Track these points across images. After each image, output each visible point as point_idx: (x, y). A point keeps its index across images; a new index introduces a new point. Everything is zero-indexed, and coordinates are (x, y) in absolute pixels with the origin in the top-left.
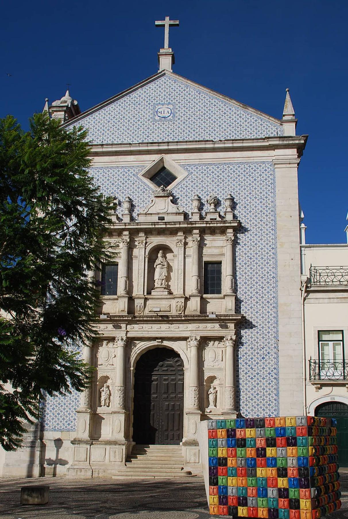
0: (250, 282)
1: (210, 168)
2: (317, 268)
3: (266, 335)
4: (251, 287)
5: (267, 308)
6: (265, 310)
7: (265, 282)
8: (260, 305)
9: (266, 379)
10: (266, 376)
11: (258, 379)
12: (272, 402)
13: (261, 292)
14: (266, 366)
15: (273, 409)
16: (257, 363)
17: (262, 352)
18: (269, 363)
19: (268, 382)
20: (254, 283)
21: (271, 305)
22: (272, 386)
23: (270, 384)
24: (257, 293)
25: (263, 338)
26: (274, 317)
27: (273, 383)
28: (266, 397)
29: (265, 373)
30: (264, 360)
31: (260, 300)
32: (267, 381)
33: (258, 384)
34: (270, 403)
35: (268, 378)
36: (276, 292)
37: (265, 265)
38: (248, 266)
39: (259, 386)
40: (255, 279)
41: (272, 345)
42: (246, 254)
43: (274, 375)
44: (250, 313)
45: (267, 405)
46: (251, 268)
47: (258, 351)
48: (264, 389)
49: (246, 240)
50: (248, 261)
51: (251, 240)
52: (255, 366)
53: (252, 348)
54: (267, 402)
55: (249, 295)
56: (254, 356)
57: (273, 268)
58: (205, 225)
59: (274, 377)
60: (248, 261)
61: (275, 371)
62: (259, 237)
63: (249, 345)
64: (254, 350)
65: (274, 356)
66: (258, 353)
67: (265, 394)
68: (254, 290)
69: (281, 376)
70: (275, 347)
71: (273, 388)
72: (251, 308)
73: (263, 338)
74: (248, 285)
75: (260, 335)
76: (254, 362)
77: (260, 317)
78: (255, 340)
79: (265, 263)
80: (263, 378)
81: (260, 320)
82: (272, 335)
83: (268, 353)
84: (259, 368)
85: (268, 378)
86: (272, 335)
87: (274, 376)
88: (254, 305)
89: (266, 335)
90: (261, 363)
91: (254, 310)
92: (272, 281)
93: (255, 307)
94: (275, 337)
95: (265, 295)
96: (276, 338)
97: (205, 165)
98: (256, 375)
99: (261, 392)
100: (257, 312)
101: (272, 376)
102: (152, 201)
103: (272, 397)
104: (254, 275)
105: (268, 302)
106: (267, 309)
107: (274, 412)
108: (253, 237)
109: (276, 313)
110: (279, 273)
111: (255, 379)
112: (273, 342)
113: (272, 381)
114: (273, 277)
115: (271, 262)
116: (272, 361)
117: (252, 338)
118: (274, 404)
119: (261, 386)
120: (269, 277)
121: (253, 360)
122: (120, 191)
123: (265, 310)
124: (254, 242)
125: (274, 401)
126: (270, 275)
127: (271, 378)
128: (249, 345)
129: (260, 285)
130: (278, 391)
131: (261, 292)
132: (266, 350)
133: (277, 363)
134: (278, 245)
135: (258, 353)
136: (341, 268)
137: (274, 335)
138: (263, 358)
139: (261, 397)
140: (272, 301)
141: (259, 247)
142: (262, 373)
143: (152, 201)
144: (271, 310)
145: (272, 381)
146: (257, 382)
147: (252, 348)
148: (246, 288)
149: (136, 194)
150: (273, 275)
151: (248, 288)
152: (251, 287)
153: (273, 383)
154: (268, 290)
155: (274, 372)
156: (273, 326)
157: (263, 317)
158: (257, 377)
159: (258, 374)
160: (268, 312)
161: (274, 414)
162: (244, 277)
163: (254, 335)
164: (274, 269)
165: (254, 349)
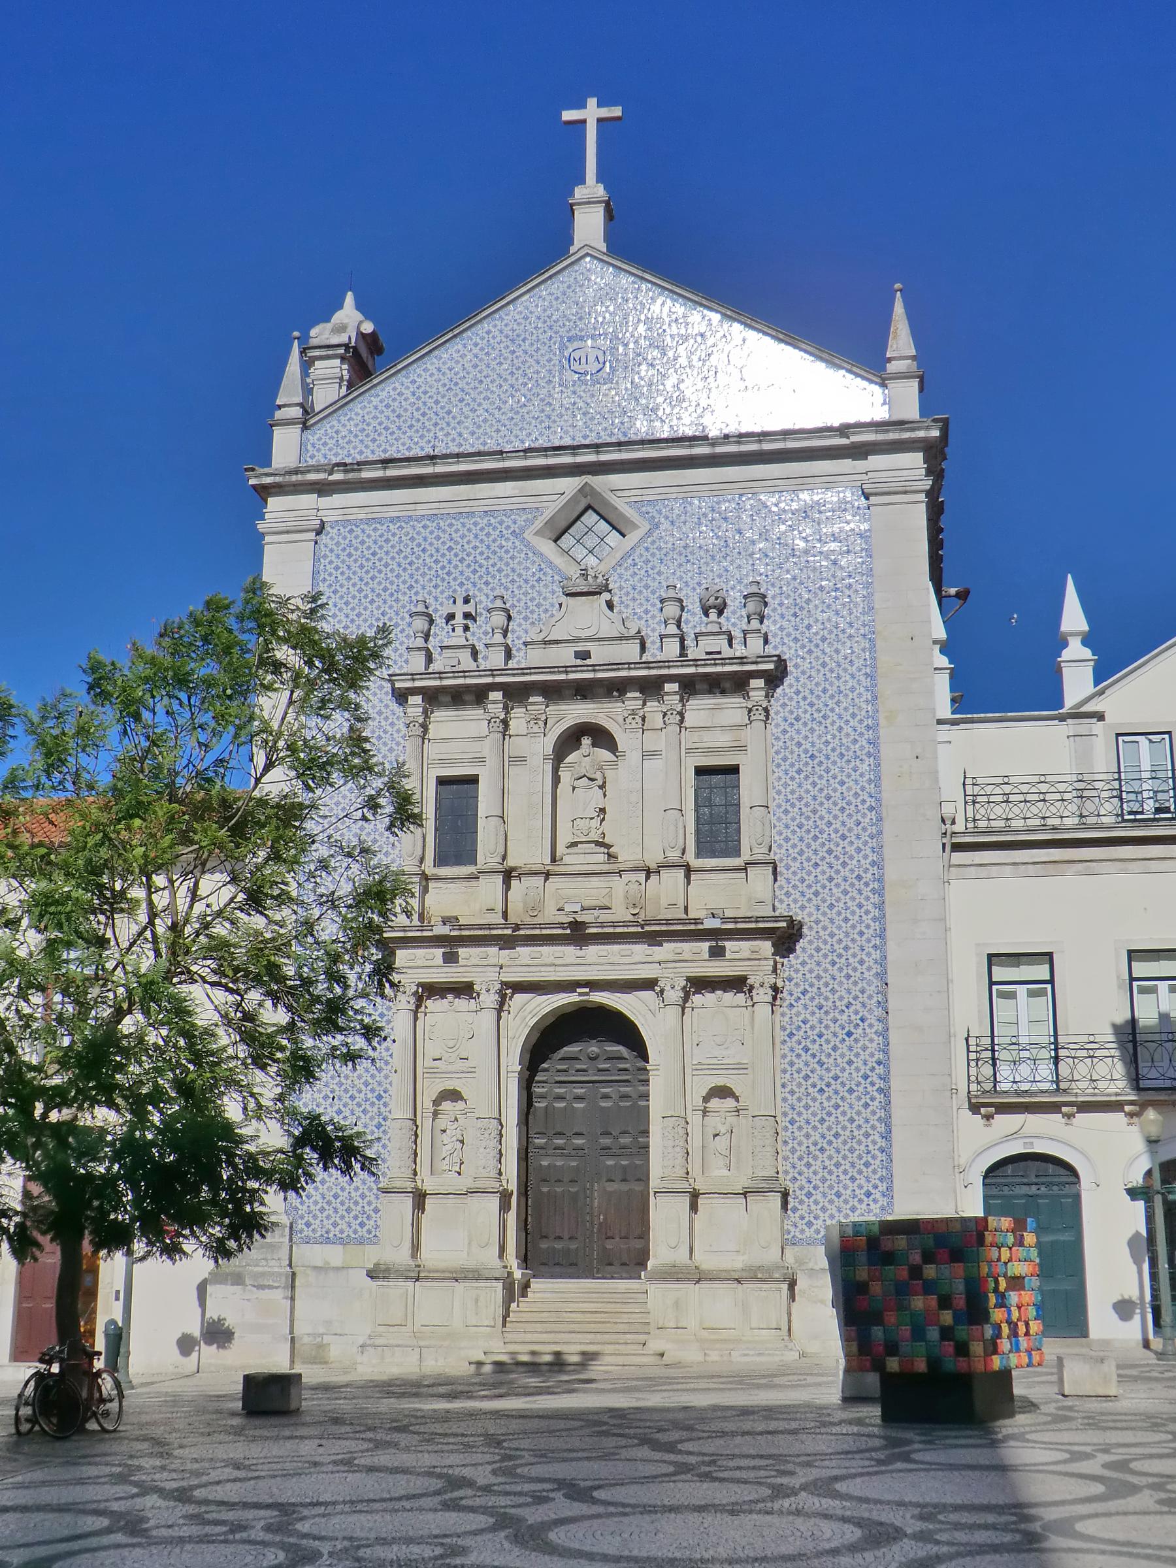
0: (811, 823)
2: (979, 781)
3: (855, 969)
4: (815, 838)
5: (855, 893)
6: (853, 899)
7: (850, 823)
8: (838, 885)
9: (856, 1094)
10: (859, 1084)
11: (836, 1092)
12: (874, 1157)
13: (840, 849)
14: (857, 1055)
15: (877, 1176)
16: (835, 1049)
17: (845, 1017)
18: (864, 1048)
19: (863, 1101)
20: (822, 824)
21: (867, 884)
22: (874, 1113)
23: (866, 1105)
24: (830, 852)
25: (848, 977)
26: (874, 919)
27: (876, 1103)
28: (859, 1142)
29: (855, 1075)
30: (852, 1038)
31: (837, 872)
32: (859, 1099)
33: (837, 1107)
34: (870, 1159)
35: (861, 1089)
36: (878, 850)
37: (849, 776)
38: (807, 777)
39: (839, 1111)
40: (824, 813)
41: (870, 997)
42: (799, 745)
43: (878, 1081)
44: (813, 910)
45: (860, 1165)
46: (814, 784)
47: (837, 1015)
48: (852, 1121)
49: (799, 707)
50: (807, 764)
51: (811, 704)
52: (829, 1055)
53: (820, 1007)
54: (860, 1157)
55: (809, 860)
56: (827, 1027)
57: (870, 781)
58: (692, 670)
59: (877, 1086)
61: (880, 1070)
62: (832, 697)
63: (812, 999)
64: (826, 1013)
65: (876, 1028)
66: (835, 1021)
67: (856, 1133)
68: (823, 845)
69: (895, 1084)
70: (879, 1002)
71: (876, 1117)
72: (816, 894)
73: (848, 977)
74: (808, 831)
75: (840, 970)
76: (825, 1047)
77: (838, 921)
78: (826, 984)
79: (848, 769)
80: (851, 1091)
81: (839, 928)
82: (869, 969)
83: (862, 1020)
84: (839, 1060)
85: (861, 1089)
86: (869, 969)
87: (880, 1084)
88: (824, 887)
89: (855, 969)
90: (843, 1048)
91: (824, 901)
92: (867, 820)
93: (827, 891)
94: (877, 974)
95: (851, 858)
96: (882, 976)
98: (833, 1082)
99: (844, 1128)
100: (831, 906)
101: (873, 1084)
102: (560, 605)
103: (874, 1143)
104: (821, 804)
105: (859, 877)
106: (858, 897)
107: (880, 1184)
108: (818, 697)
109: (881, 906)
110: (885, 795)
111: (830, 1092)
112: (873, 988)
113: (873, 1099)
114: (871, 808)
115: (865, 767)
116: (871, 1041)
117: (819, 977)
118: (878, 1162)
119: (844, 1113)
120: (860, 807)
121: (823, 1039)
122: (481, 577)
123: (853, 899)
124: (819, 711)
125: (879, 1154)
126: (864, 802)
127: (870, 1089)
128: (812, 999)
129: (836, 831)
130: (888, 1126)
131: (840, 849)
132: (857, 1013)
133: (885, 1049)
134: (882, 722)
135: (835, 1021)
136: (1043, 779)
137: (876, 968)
138: (849, 1034)
139: (845, 1143)
140: (869, 875)
141: (833, 723)
142: (846, 1074)
143: (560, 605)
144: (868, 898)
145: (873, 1099)
146: (833, 1101)
147: (820, 1007)
148: (801, 839)
149: (520, 587)
150: (871, 802)
151: (808, 838)
152: (815, 838)
153: (876, 1103)
154: (858, 843)
155: (877, 1071)
156: (873, 943)
157: (846, 920)
158: (833, 1087)
159: (836, 1078)
160: (860, 906)
161: (880, 1189)
163: (826, 971)
164: (873, 786)
165: (825, 1009)
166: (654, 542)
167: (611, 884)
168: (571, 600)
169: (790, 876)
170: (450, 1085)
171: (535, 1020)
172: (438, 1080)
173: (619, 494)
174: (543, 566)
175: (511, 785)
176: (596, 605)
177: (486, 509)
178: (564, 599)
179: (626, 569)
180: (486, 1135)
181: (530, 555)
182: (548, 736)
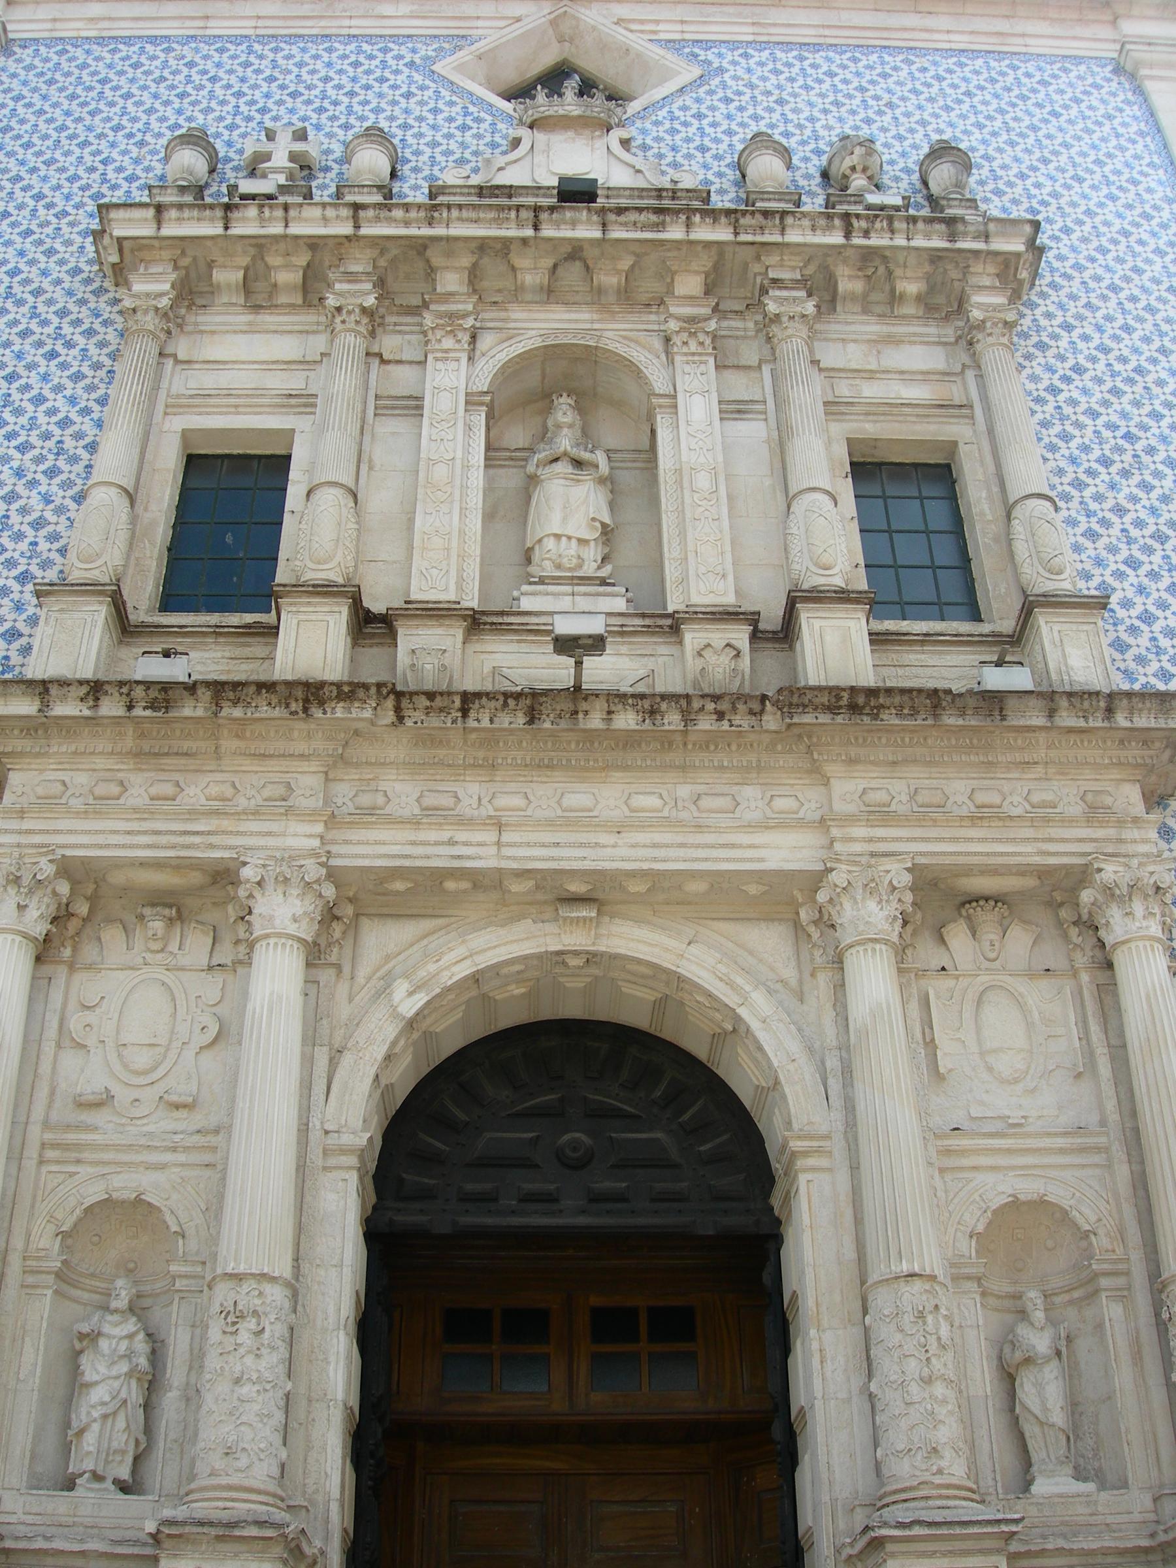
1: (819, 58)
60: (1120, 450)
97: (787, 46)
162: (1115, 531)
166: (711, 93)
167: (650, 663)
168: (540, 137)
169: (1132, 665)
170: (124, 1185)
171: (421, 999)
172: (84, 1171)
173: (634, 27)
174: (472, 109)
175: (378, 453)
176: (600, 144)
177: (353, 32)
178: (524, 132)
179: (657, 123)
180: (244, 1337)
181: (444, 93)
182: (481, 363)
